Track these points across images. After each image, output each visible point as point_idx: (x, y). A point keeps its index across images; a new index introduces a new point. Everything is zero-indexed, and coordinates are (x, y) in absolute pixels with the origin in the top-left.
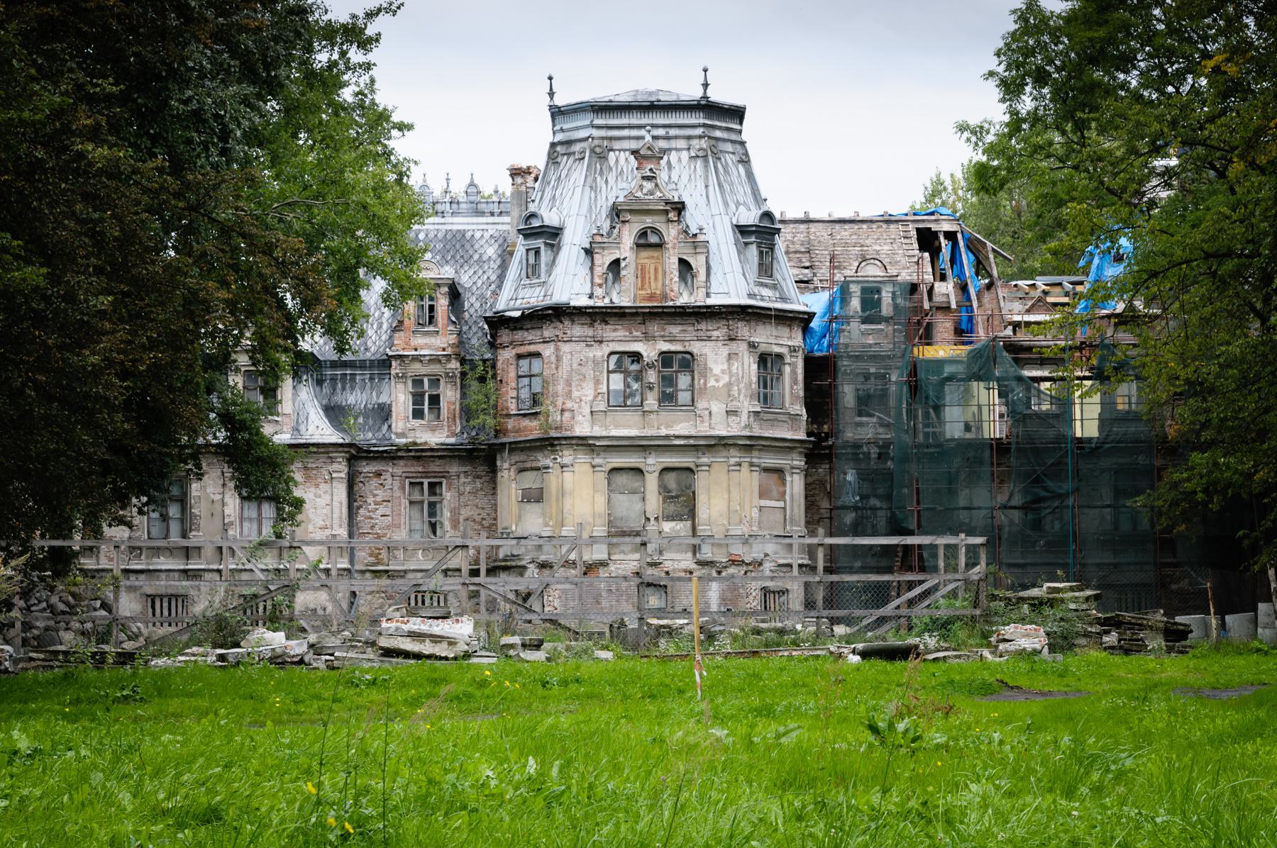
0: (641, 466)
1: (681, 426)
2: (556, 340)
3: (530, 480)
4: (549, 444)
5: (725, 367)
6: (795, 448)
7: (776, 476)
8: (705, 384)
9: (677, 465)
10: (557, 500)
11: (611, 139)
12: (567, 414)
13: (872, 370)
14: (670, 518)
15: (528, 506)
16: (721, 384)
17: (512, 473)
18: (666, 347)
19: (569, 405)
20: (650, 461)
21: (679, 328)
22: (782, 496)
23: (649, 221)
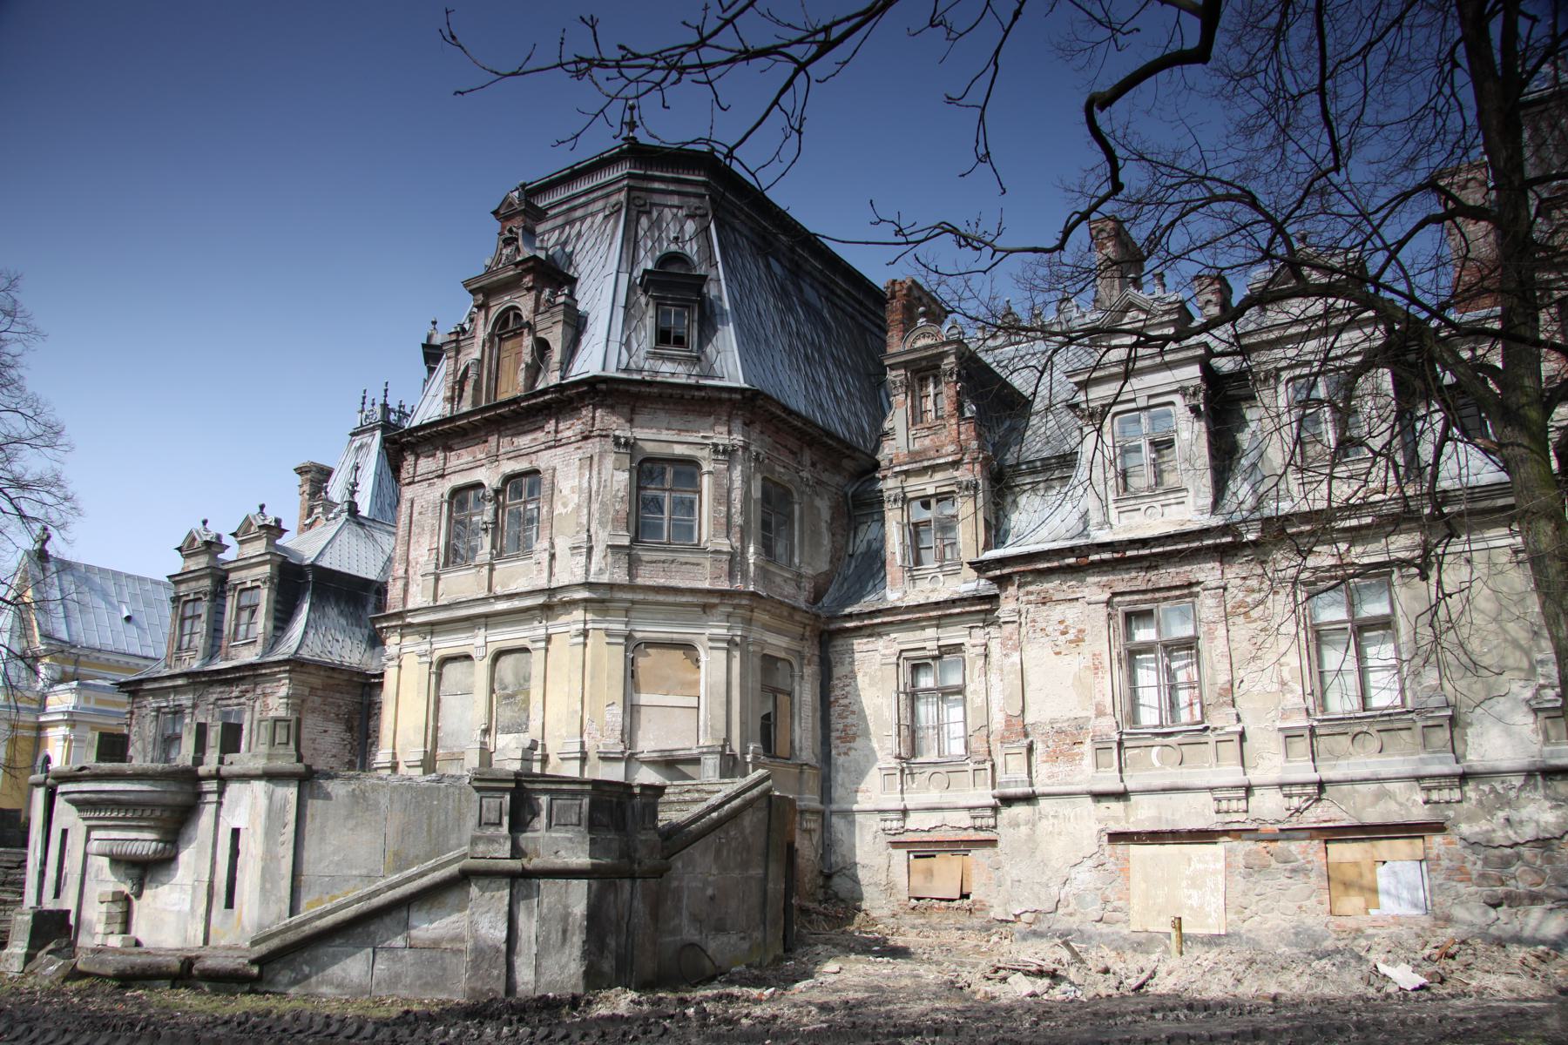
1: (521, 576)
6: (714, 606)
7: (679, 654)
13: (931, 490)
14: (508, 730)
16: (570, 509)
18: (509, 467)
20: (480, 641)
21: (530, 437)
22: (691, 687)
23: (506, 300)
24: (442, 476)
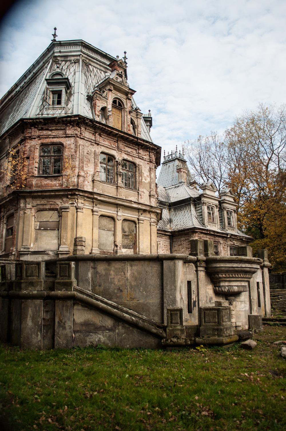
0: (115, 216)
2: (75, 136)
3: (51, 217)
4: (72, 193)
5: (148, 174)
8: (142, 180)
9: (130, 218)
10: (72, 229)
11: (90, 60)
12: (81, 179)
15: (44, 233)
16: (147, 181)
17: (33, 211)
18: (126, 157)
19: (82, 173)
24: (98, 144)
